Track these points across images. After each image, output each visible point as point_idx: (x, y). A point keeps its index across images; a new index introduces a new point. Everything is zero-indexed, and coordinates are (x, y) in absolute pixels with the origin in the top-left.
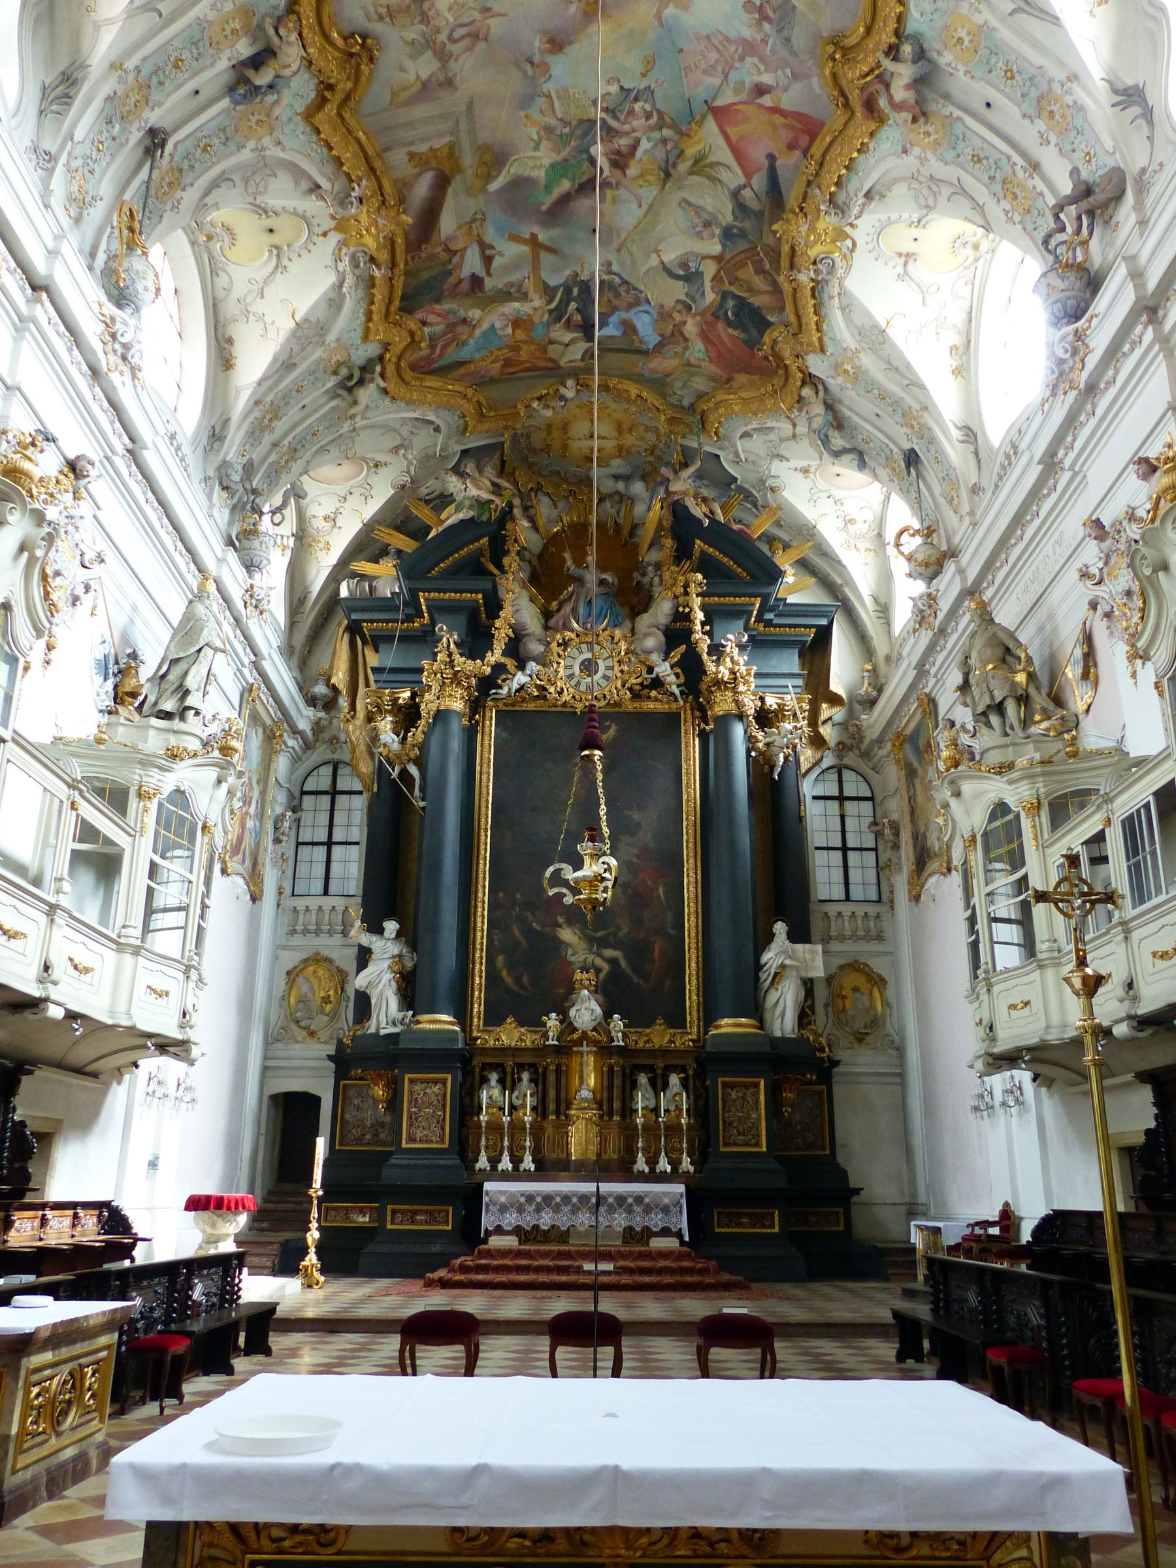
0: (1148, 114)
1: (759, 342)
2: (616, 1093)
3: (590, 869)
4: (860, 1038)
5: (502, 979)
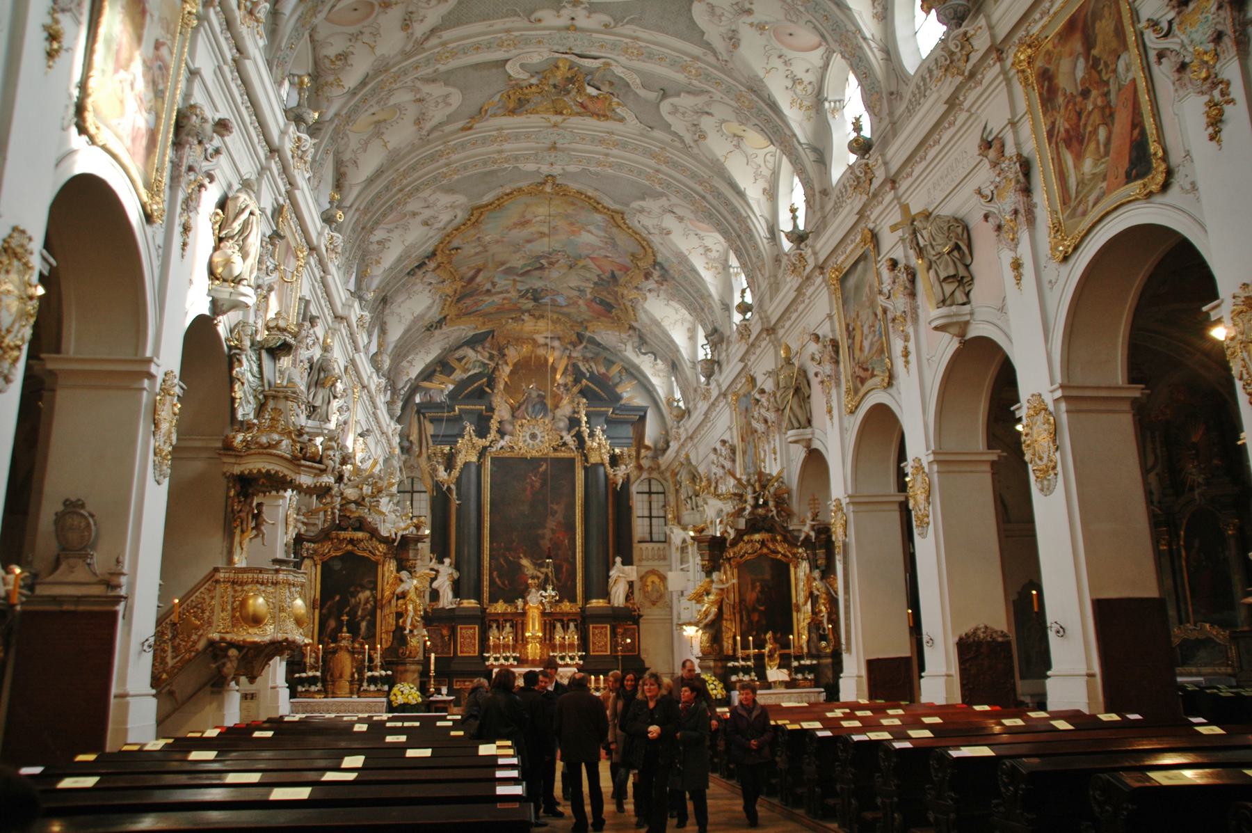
2: (548, 632)
4: (654, 603)
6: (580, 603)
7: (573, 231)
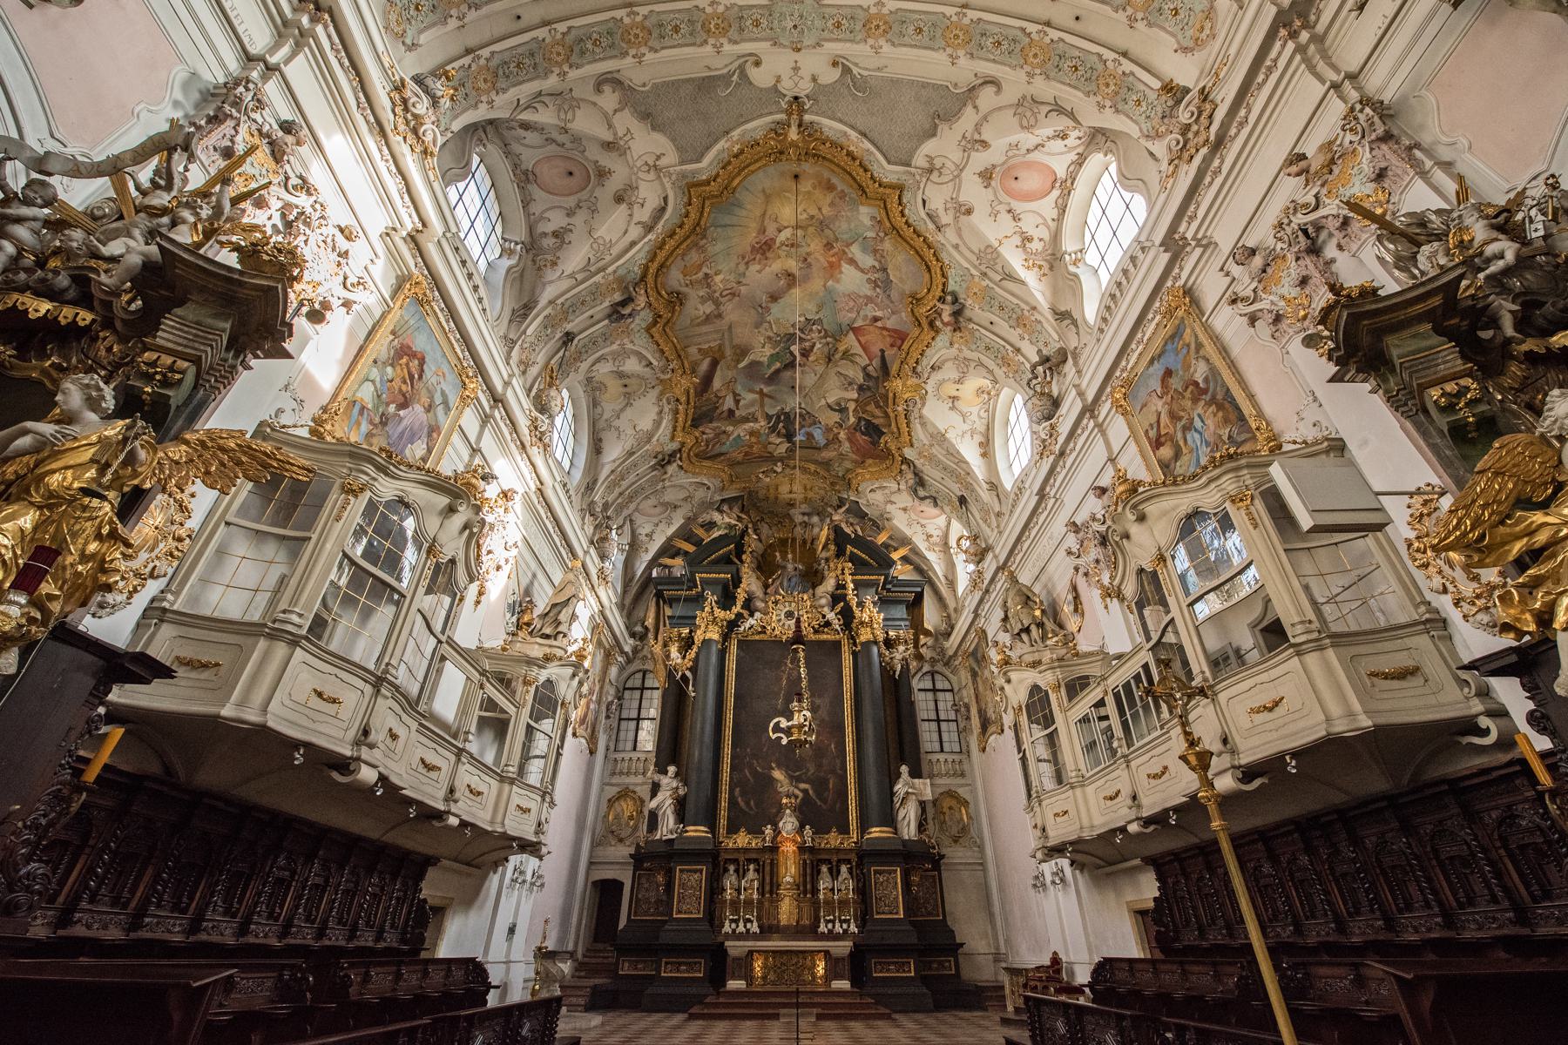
0: (1075, 323)
1: (878, 443)
3: (798, 719)
4: (956, 840)
5: (737, 803)
6: (854, 837)
7: (831, 265)
